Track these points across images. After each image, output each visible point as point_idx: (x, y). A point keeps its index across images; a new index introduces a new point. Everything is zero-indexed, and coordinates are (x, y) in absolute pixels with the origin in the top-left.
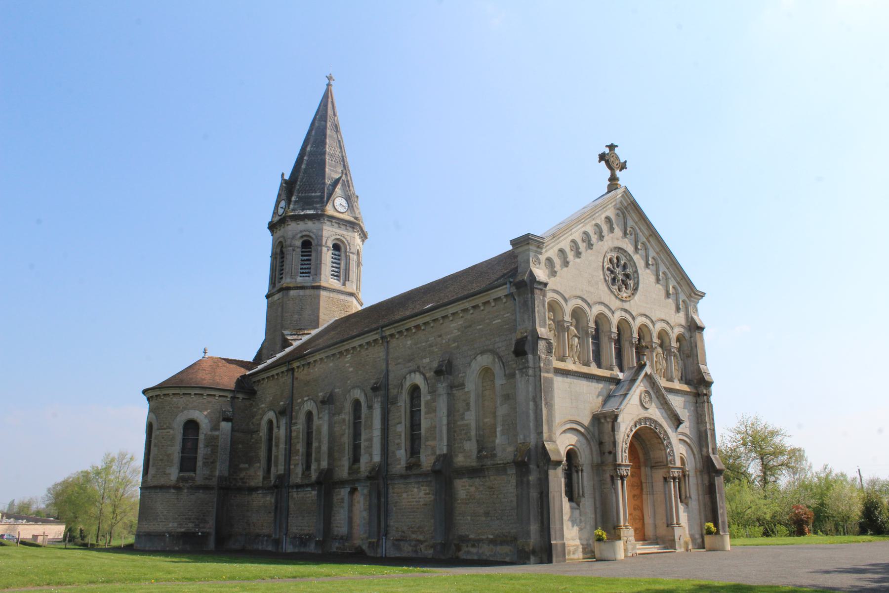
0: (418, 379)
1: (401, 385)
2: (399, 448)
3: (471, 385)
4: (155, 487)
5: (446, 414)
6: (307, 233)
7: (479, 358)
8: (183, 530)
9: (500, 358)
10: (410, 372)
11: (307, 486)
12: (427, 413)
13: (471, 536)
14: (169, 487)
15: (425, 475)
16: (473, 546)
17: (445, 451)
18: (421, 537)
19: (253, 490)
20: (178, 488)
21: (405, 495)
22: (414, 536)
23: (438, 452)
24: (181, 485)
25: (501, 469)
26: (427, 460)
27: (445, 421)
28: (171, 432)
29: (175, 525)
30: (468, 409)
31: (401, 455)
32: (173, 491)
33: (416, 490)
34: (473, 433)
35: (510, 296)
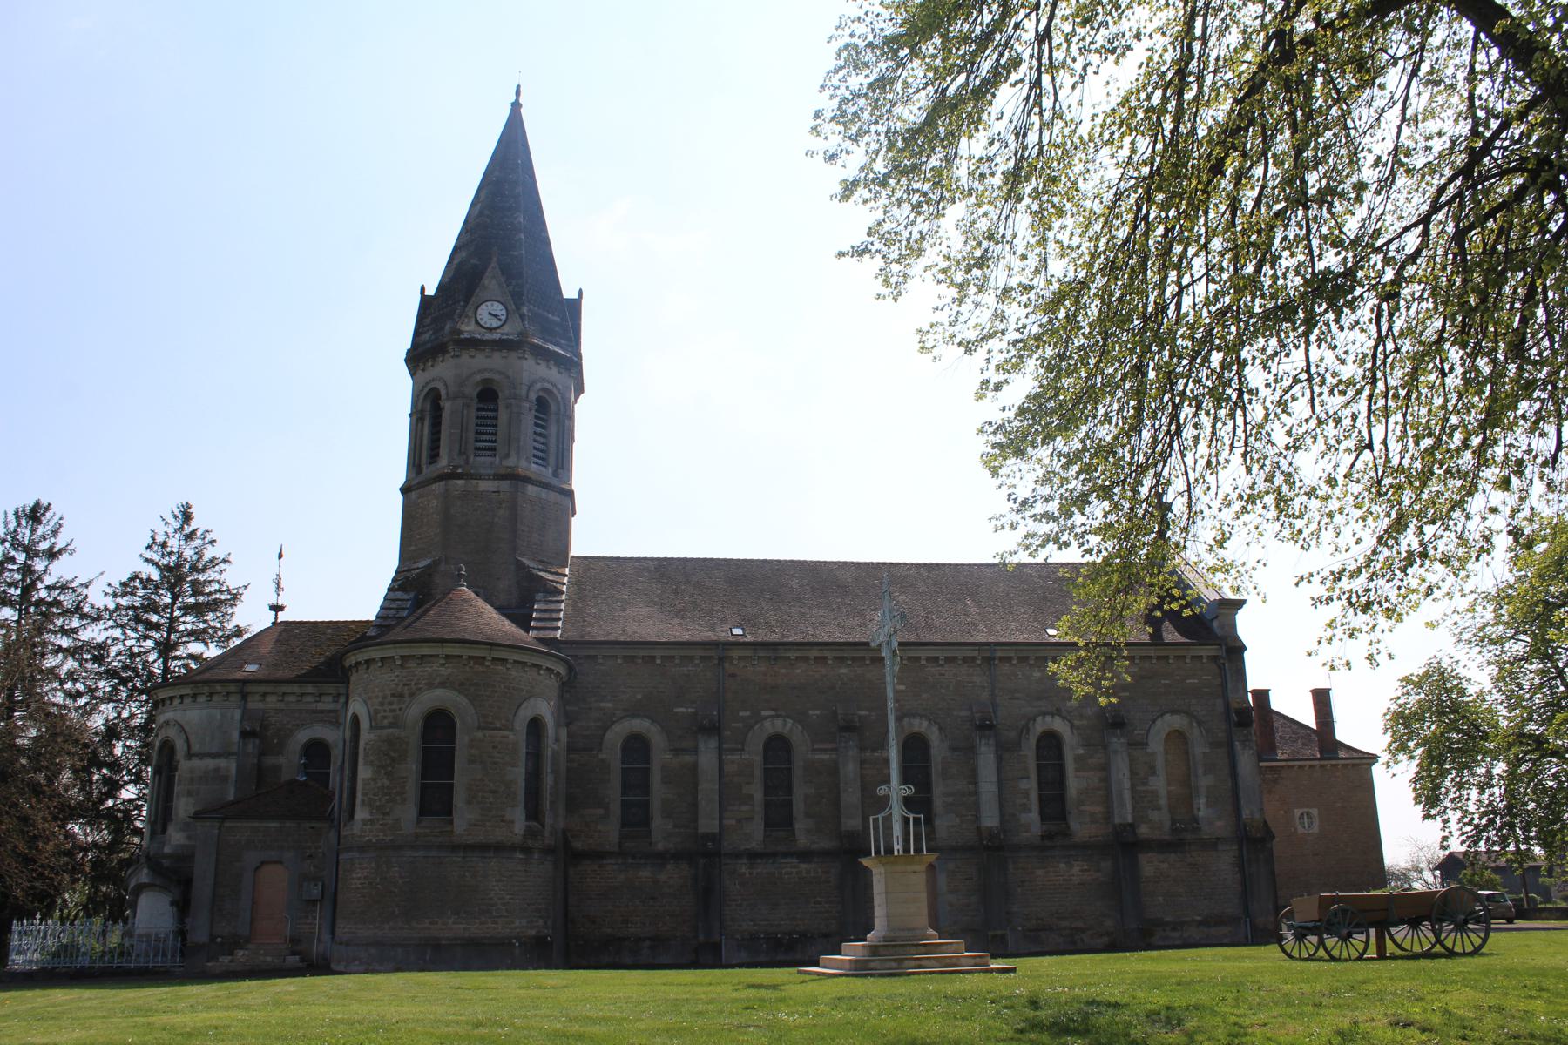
0: (1058, 725)
1: (1026, 728)
2: (1026, 809)
3: (1156, 745)
4: (483, 848)
5: (1127, 774)
6: (549, 386)
7: (1167, 717)
8: (533, 932)
9: (1199, 723)
10: (1044, 714)
11: (785, 855)
12: (1077, 770)
13: (1168, 919)
14: (513, 848)
15: (1084, 846)
16: (1174, 929)
17: (1130, 820)
18: (1079, 924)
19: (598, 855)
20: (527, 850)
21: (1040, 872)
22: (1065, 924)
23: (1117, 820)
24: (530, 843)
25: (1212, 844)
26: (1082, 828)
27: (1127, 784)
28: (512, 736)
29: (524, 922)
30: (1154, 774)
31: (1032, 818)
32: (519, 855)
33: (1062, 866)
34: (1163, 802)
35: (1214, 658)
